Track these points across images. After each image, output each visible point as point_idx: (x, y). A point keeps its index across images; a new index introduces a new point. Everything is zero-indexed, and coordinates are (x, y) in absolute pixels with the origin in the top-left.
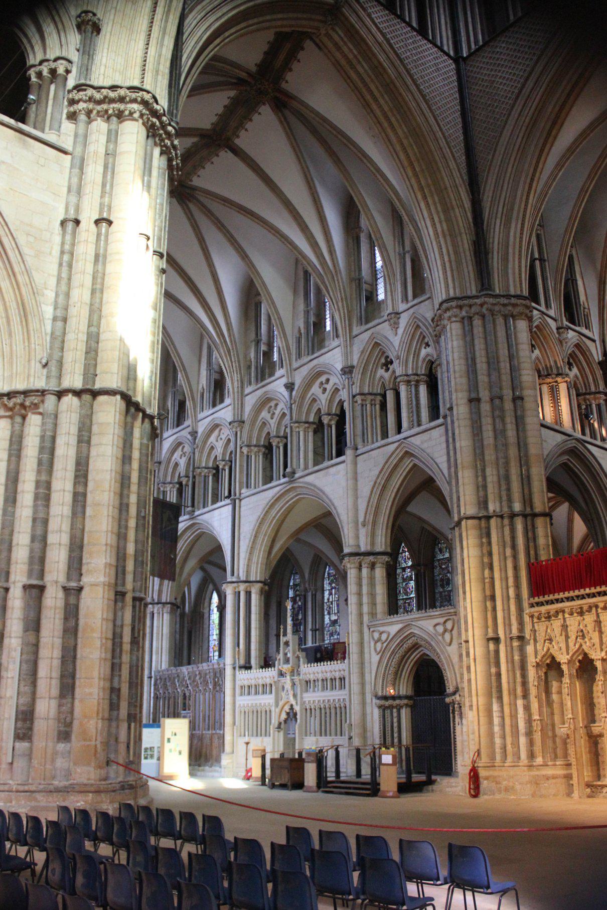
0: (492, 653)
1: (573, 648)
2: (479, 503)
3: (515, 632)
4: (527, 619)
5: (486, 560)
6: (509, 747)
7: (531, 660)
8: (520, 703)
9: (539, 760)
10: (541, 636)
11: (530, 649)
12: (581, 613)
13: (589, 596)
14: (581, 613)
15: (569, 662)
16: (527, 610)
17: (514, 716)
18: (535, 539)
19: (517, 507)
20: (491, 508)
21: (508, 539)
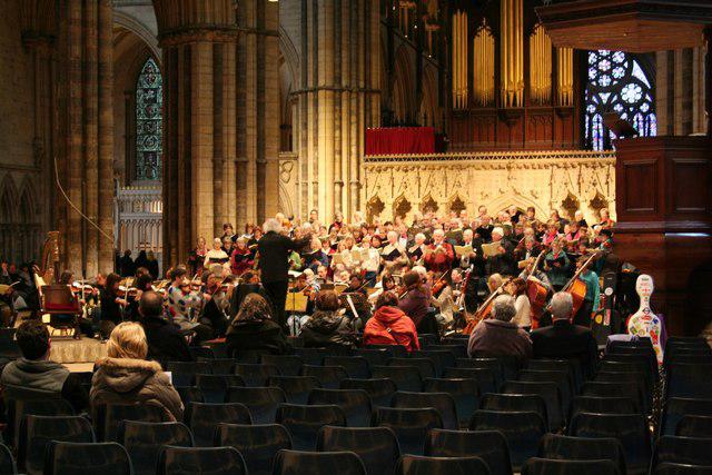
0: (337, 194)
1: (397, 194)
2: (335, 78)
3: (354, 179)
4: (362, 169)
5: (337, 123)
7: (363, 201)
10: (371, 184)
11: (362, 191)
12: (406, 171)
13: (413, 159)
14: (406, 171)
16: (363, 164)
18: (371, 109)
19: (362, 84)
20: (344, 83)
21: (354, 108)
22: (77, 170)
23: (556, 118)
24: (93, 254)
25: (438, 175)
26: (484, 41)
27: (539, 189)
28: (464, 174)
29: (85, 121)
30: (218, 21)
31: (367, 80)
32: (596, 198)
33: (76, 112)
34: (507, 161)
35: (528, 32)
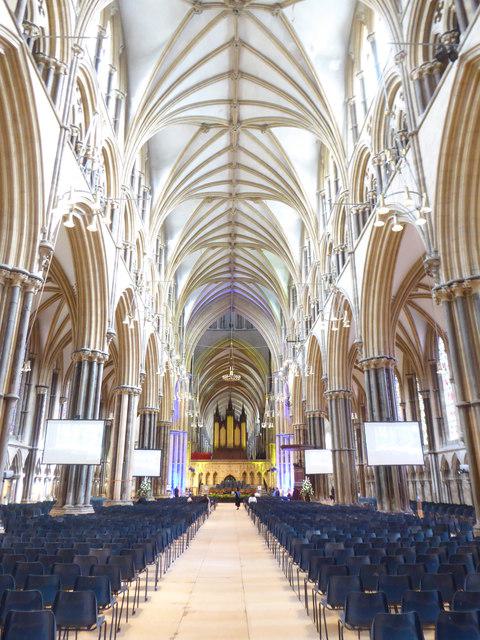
26: (223, 429)
35: (234, 428)
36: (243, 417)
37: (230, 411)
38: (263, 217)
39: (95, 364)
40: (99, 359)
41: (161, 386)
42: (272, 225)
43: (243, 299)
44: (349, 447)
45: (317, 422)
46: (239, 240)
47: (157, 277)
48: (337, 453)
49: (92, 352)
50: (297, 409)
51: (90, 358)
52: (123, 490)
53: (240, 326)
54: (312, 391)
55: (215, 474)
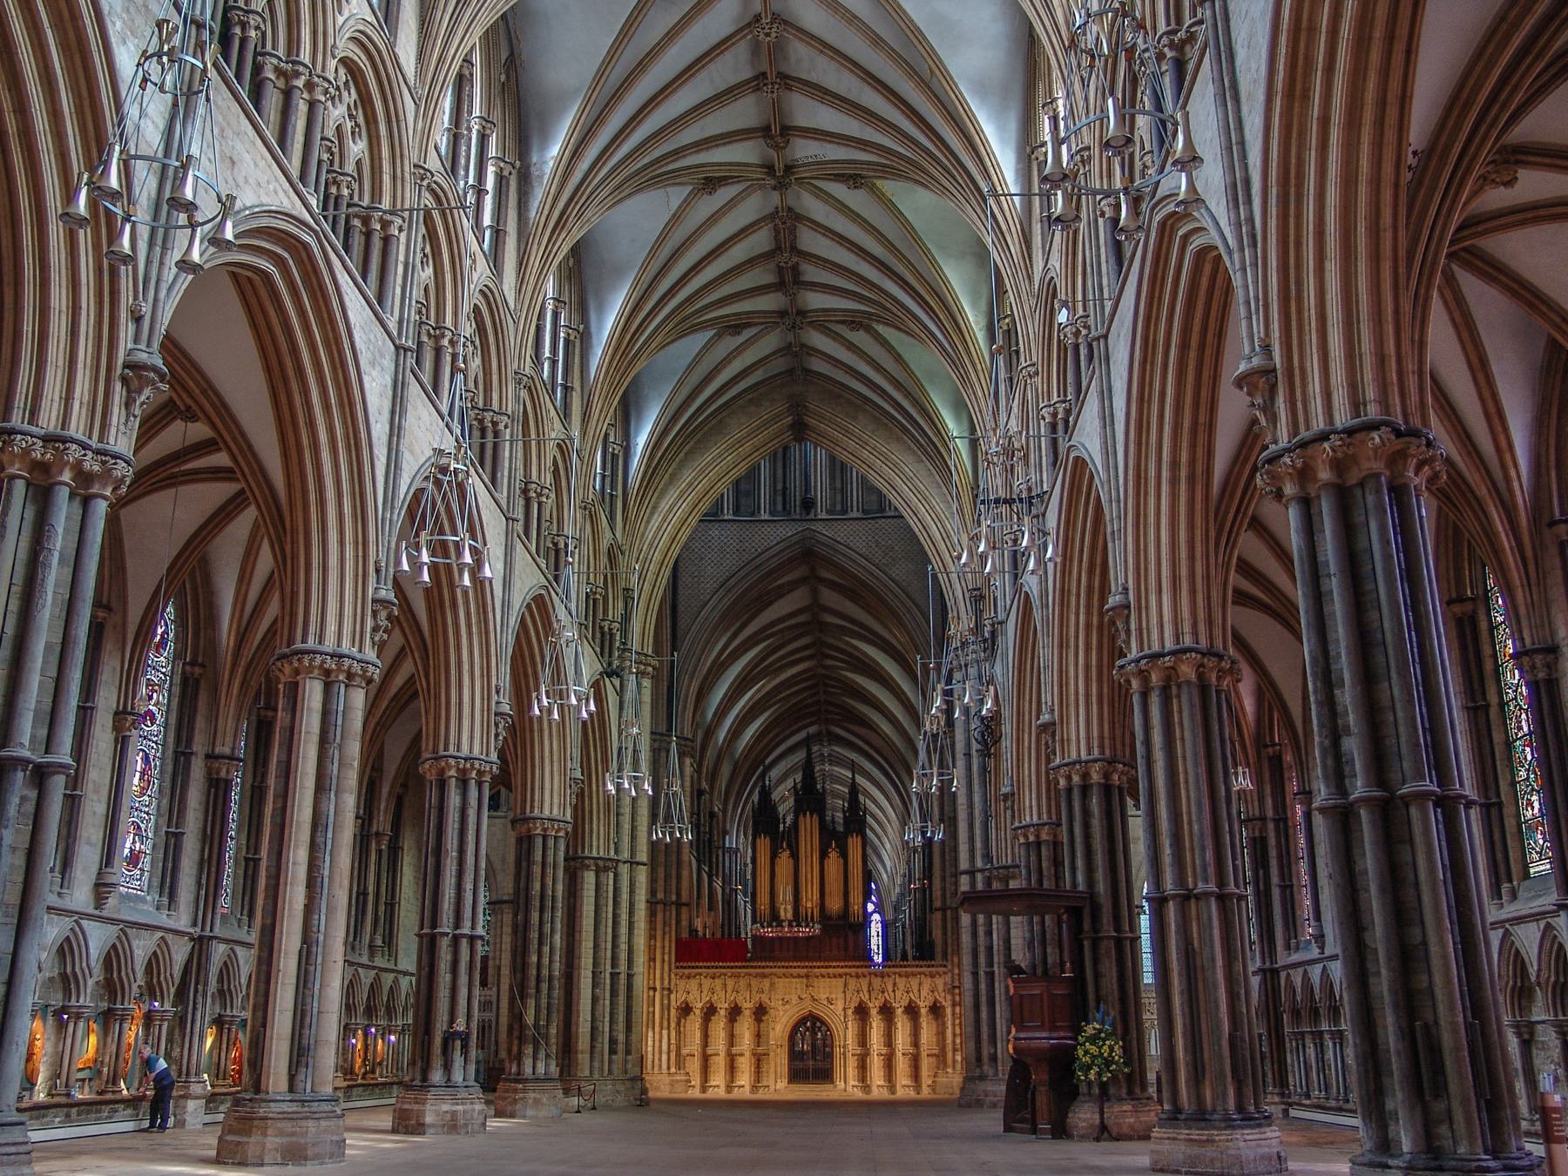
6: (656, 1061)
7: (673, 1003)
8: (665, 1032)
9: (673, 1070)
11: (673, 996)
15: (702, 1009)
16: (674, 970)
17: (661, 1041)
19: (674, 898)
20: (660, 896)
22: (533, 983)
23: (850, 934)
24: (542, 1054)
25: (743, 982)
26: (784, 860)
27: (833, 996)
28: (766, 983)
29: (540, 944)
30: (601, 854)
31: (678, 894)
32: (885, 1004)
33: (534, 935)
34: (805, 970)
35: (823, 855)
36: (856, 820)
37: (810, 798)
38: (877, 41)
39: (64, 492)
40: (84, 478)
41: (502, 675)
42: (912, 72)
43: (838, 394)
44: (1221, 883)
45: (1095, 803)
46: (804, 150)
47: (480, 273)
48: (1171, 909)
49: (48, 439)
50: (1029, 769)
51: (42, 468)
52: (301, 1054)
53: (840, 509)
54: (1077, 683)
55: (760, 1012)
